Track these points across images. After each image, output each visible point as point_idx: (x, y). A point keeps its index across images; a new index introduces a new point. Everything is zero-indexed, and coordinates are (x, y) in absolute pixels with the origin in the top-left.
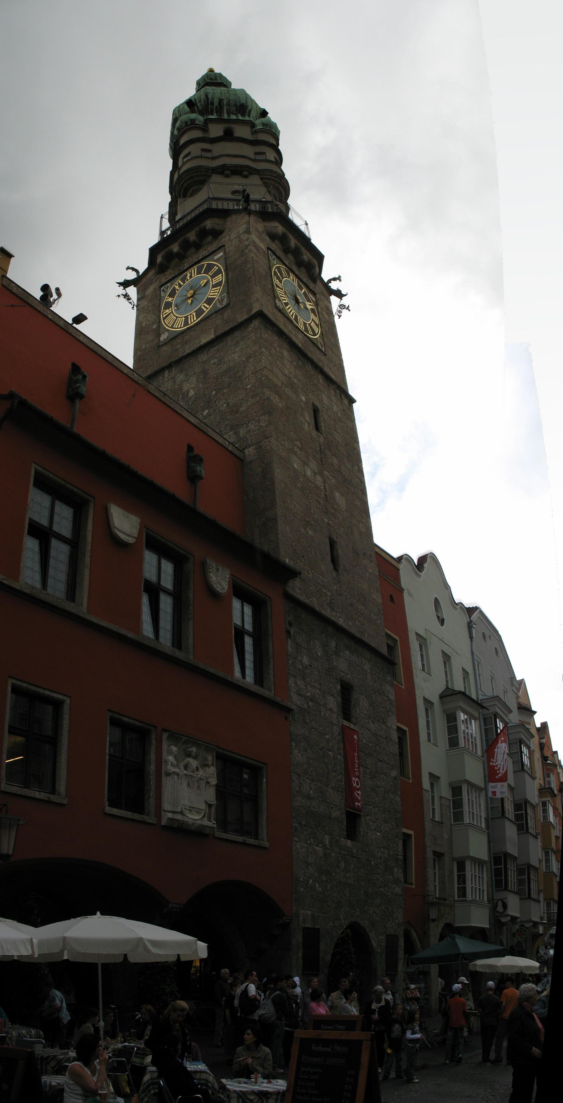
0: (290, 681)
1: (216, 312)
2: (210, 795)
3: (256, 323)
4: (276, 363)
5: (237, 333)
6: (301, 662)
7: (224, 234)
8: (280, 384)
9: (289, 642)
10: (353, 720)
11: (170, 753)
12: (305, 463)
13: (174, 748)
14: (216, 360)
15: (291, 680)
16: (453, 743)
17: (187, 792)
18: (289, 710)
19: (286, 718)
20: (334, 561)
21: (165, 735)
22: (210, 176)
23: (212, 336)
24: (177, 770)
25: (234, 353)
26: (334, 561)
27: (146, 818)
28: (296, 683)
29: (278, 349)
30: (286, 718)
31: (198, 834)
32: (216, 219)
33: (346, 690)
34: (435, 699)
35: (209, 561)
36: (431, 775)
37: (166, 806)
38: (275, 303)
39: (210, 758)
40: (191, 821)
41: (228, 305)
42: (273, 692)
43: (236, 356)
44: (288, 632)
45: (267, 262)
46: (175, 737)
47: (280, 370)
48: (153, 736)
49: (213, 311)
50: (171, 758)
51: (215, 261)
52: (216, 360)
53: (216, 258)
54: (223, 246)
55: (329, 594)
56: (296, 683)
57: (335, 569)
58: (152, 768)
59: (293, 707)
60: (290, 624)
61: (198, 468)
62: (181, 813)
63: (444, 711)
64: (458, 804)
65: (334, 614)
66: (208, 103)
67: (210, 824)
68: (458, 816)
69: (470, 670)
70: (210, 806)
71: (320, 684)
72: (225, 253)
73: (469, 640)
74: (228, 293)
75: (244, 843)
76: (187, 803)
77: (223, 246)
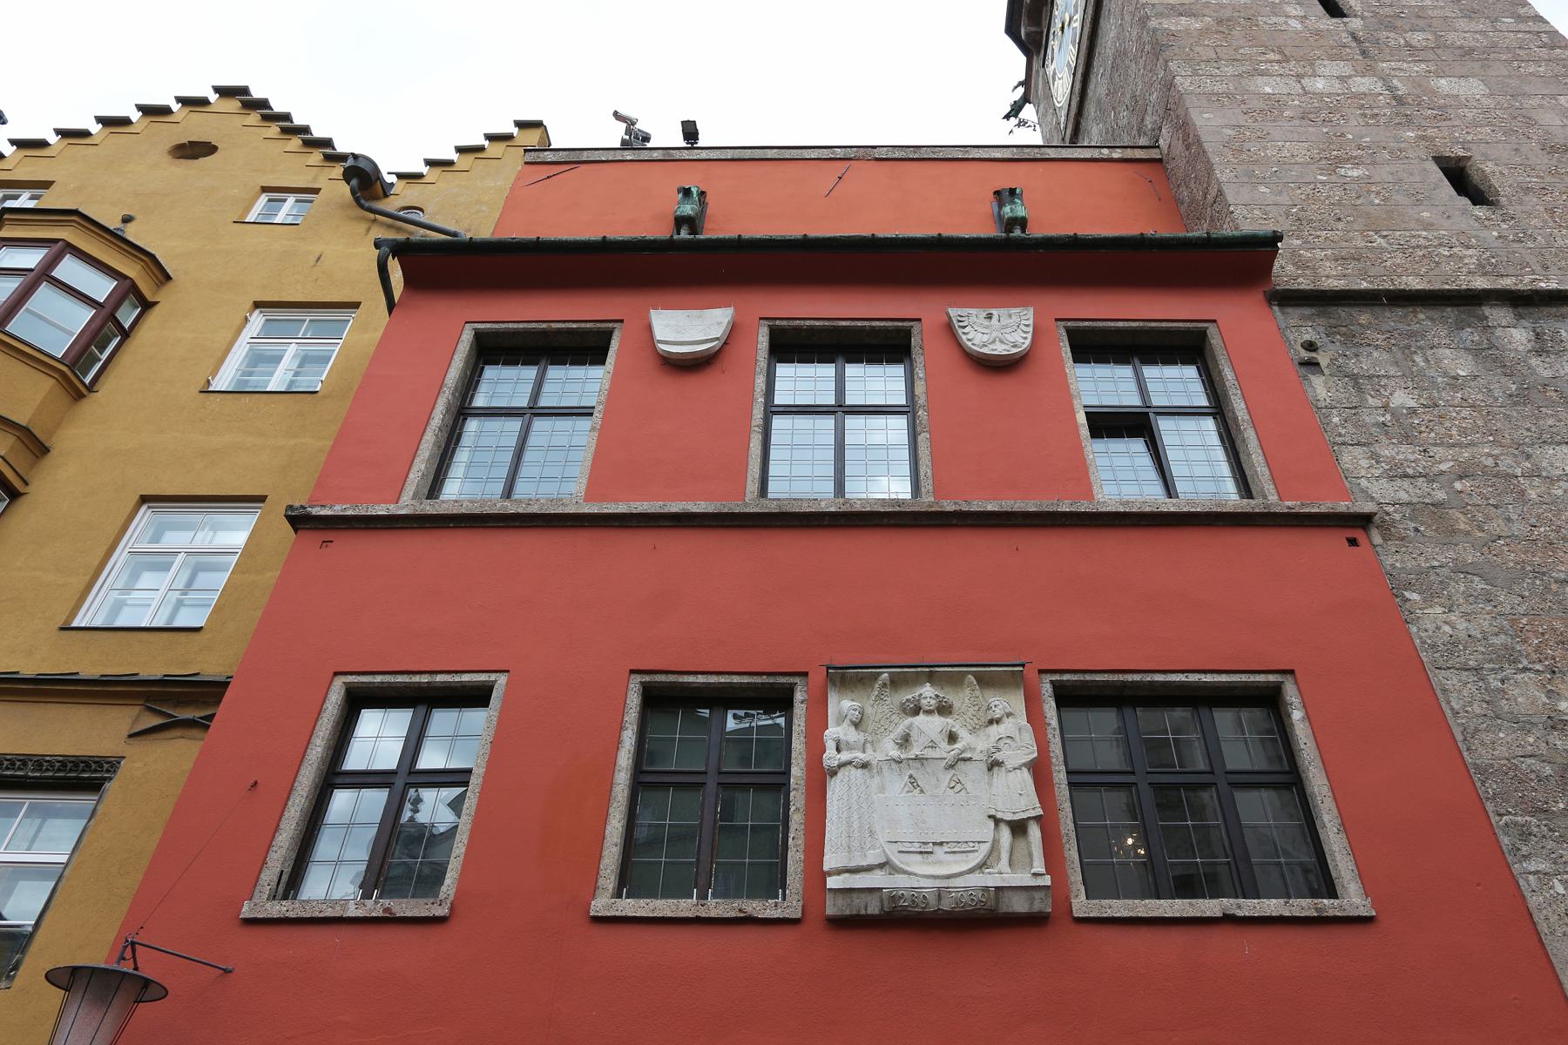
6: (1386, 407)
28: (1376, 457)
56: (1376, 457)
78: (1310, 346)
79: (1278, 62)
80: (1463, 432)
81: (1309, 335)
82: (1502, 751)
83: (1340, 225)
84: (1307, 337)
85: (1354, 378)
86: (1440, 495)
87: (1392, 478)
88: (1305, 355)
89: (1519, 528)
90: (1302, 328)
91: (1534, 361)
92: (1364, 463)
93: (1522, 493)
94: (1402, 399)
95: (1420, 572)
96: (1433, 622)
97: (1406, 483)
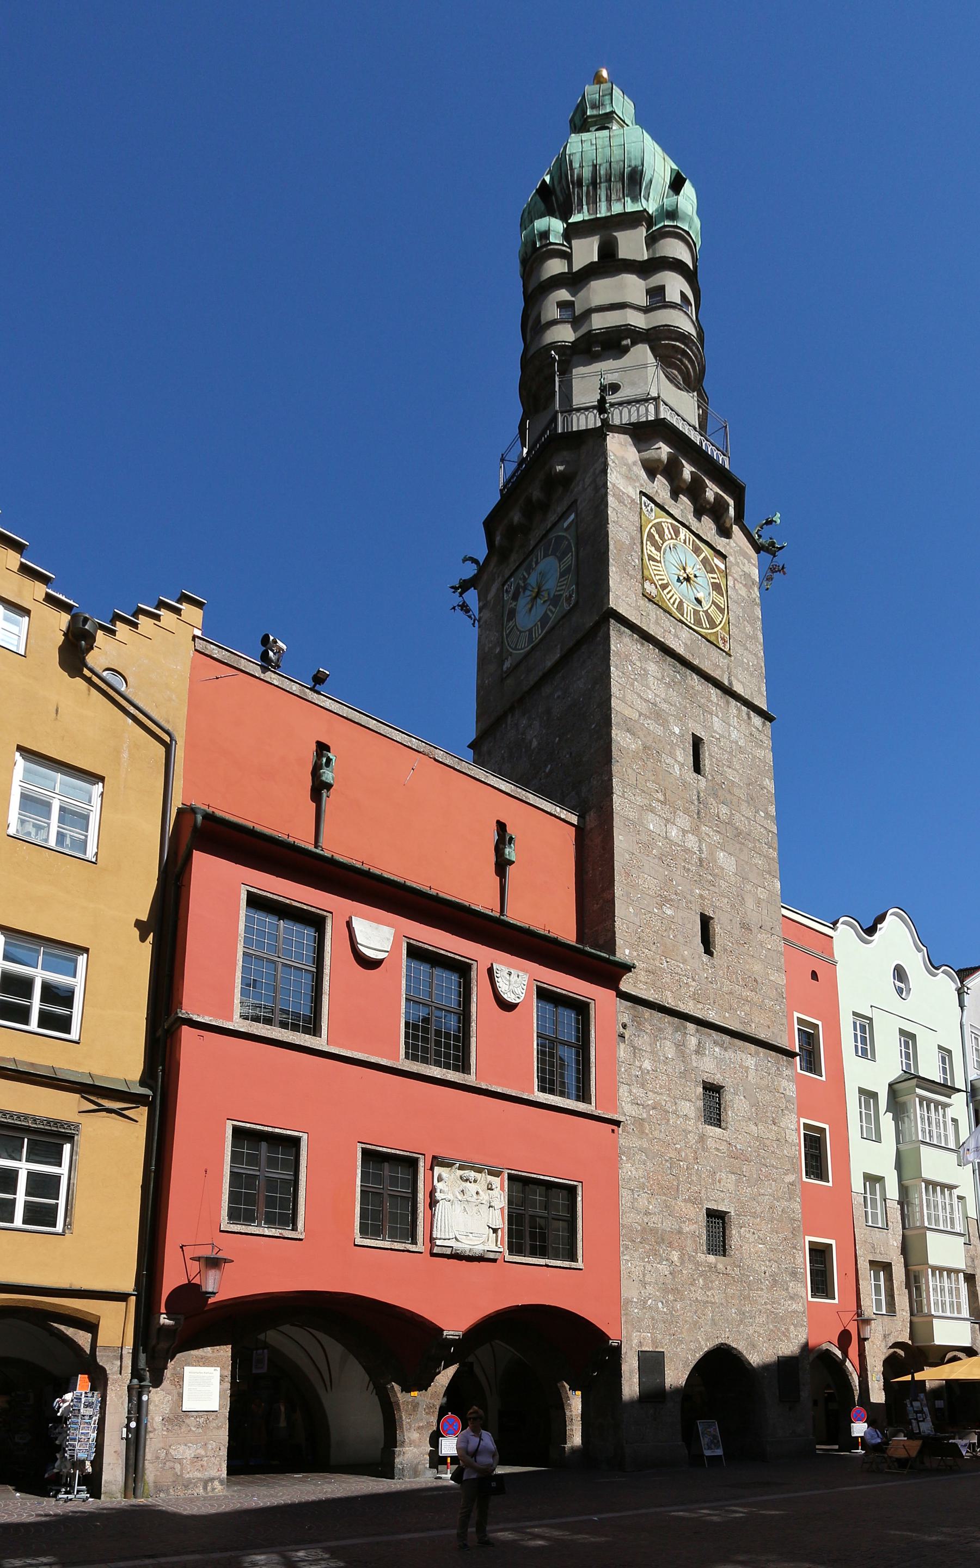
0: (621, 1090)
1: (563, 617)
4: (632, 685)
6: (640, 1067)
8: (635, 716)
14: (559, 693)
15: (623, 1091)
18: (617, 1123)
19: (613, 1131)
28: (630, 1092)
29: (638, 664)
30: (613, 1131)
38: (644, 589)
41: (577, 603)
42: (593, 1104)
44: (622, 1036)
45: (637, 519)
52: (559, 693)
53: (565, 525)
55: (693, 984)
56: (630, 1092)
57: (708, 951)
60: (624, 1026)
65: (700, 1006)
71: (670, 1090)
72: (576, 516)
74: (577, 585)
79: (659, 801)
80: (661, 1087)
81: (625, 1019)
82: (630, 1220)
83: (654, 948)
84: (625, 1020)
86: (645, 1116)
87: (632, 1104)
88: (622, 1030)
89: (662, 1136)
90: (624, 1012)
91: (693, 1057)
92: (626, 1094)
93: (668, 1120)
94: (647, 1065)
95: (629, 1148)
96: (628, 1170)
97: (635, 1107)
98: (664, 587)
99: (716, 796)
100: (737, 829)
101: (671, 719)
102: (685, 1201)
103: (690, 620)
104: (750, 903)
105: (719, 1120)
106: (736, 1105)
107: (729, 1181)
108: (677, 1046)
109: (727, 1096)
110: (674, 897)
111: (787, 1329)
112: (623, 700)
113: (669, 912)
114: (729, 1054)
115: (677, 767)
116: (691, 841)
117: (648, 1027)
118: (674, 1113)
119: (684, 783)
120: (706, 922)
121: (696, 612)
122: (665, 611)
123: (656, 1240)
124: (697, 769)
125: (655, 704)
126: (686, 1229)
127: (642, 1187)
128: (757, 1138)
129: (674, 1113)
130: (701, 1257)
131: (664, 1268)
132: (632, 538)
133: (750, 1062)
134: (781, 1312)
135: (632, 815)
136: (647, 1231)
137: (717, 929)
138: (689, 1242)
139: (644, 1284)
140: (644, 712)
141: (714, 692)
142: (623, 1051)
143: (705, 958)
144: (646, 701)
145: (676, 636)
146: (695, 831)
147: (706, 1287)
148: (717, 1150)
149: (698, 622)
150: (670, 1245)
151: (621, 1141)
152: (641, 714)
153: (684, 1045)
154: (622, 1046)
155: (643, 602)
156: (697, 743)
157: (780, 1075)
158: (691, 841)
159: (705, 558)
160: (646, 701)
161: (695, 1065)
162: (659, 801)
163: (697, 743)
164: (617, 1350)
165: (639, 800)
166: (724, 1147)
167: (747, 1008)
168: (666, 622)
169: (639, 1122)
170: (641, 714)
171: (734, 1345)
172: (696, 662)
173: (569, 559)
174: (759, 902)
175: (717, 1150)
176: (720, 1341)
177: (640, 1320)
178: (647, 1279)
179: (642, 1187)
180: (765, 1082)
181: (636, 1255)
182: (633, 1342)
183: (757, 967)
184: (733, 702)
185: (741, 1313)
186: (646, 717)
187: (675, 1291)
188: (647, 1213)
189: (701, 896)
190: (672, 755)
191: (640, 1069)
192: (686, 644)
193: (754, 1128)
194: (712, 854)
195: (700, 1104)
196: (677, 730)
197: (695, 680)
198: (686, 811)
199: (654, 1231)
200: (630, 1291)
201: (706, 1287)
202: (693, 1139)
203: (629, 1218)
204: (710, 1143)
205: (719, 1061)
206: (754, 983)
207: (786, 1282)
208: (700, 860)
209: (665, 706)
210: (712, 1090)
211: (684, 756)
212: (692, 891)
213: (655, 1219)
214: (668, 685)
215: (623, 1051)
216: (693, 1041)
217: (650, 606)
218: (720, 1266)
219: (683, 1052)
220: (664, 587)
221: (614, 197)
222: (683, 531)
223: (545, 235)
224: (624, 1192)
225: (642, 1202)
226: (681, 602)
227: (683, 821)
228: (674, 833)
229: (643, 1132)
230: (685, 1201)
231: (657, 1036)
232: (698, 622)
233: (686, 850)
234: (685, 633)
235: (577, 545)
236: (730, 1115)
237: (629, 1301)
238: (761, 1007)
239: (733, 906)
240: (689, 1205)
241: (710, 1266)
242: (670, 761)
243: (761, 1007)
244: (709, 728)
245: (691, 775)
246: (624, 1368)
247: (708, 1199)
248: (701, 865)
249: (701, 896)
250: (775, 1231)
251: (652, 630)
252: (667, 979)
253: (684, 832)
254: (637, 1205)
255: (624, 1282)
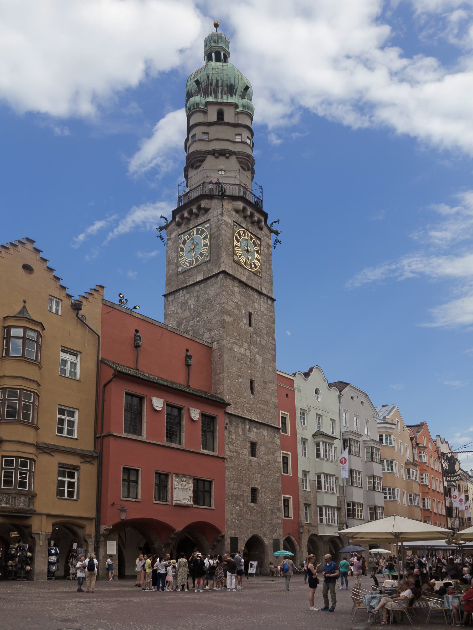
2: (191, 494)
3: (221, 276)
5: (213, 279)
7: (211, 211)
8: (231, 309)
9: (226, 431)
10: (257, 456)
11: (176, 481)
12: (241, 346)
13: (177, 480)
15: (226, 447)
16: (318, 456)
17: (182, 492)
18: (224, 458)
20: (252, 389)
21: (174, 475)
22: (206, 157)
23: (202, 278)
24: (178, 487)
25: (212, 290)
26: (252, 389)
27: (167, 503)
28: (228, 447)
31: (186, 507)
32: (206, 200)
33: (253, 445)
34: (309, 437)
35: (191, 408)
36: (303, 471)
37: (174, 499)
39: (190, 481)
40: (183, 503)
41: (210, 260)
43: (211, 292)
44: (226, 428)
46: (177, 475)
47: (232, 300)
48: (170, 476)
49: (203, 262)
50: (176, 483)
51: (206, 228)
54: (210, 220)
57: (252, 393)
58: (169, 486)
59: (226, 457)
61: (190, 361)
62: (180, 500)
63: (315, 442)
64: (319, 482)
66: (209, 84)
67: (190, 503)
68: (320, 488)
69: (336, 418)
70: (191, 497)
73: (338, 403)
74: (210, 253)
75: (204, 508)
76: (182, 497)
77: (210, 220)
78: (227, 424)
79: (238, 339)
85: (230, 431)
94: (233, 437)
98: (240, 256)
99: (256, 333)
100: (263, 345)
101: (242, 308)
102: (245, 484)
103: (248, 267)
104: (266, 373)
105: (255, 454)
106: (261, 449)
107: (258, 476)
108: (243, 429)
109: (258, 447)
110: (242, 374)
111: (276, 529)
112: (227, 304)
113: (240, 380)
114: (259, 431)
115: (244, 325)
116: (248, 353)
117: (234, 423)
118: (241, 453)
119: (246, 331)
120: (252, 382)
121: (251, 264)
122: (240, 266)
123: (236, 498)
124: (250, 325)
125: (237, 303)
126: (245, 495)
127: (232, 480)
128: (268, 461)
129: (241, 453)
130: (249, 504)
131: (238, 508)
132: (230, 240)
133: (266, 433)
134: (274, 523)
135: (229, 346)
136: (233, 495)
137: (256, 385)
138: (246, 499)
139: (232, 514)
140: (234, 306)
141: (256, 295)
142: (226, 433)
143: (252, 396)
144: (234, 302)
145: (244, 274)
146: (249, 348)
147: (251, 515)
148: (255, 466)
149: (251, 268)
150: (240, 500)
151: (226, 465)
152: (232, 308)
153: (245, 429)
154: (226, 431)
155: (234, 264)
156: (250, 314)
157: (275, 437)
158: (248, 353)
159: (254, 241)
160: (234, 302)
161: (248, 435)
162: (238, 339)
163: (250, 314)
164: (223, 537)
165: (232, 340)
166: (257, 465)
167: (265, 413)
168: (241, 270)
169: (231, 457)
170: (232, 308)
171: (259, 535)
172: (250, 284)
173: (207, 241)
174: (269, 372)
175: (255, 466)
176: (255, 533)
177: (231, 526)
178: (233, 512)
179: (232, 480)
180: (270, 440)
181: (230, 504)
182: (229, 533)
183: (268, 397)
184: (262, 299)
185: (262, 523)
186: (235, 309)
187: (241, 516)
188: (233, 489)
189: (251, 373)
190: (242, 321)
191: (232, 440)
192: (247, 277)
193: (266, 457)
194: (254, 356)
195: (250, 449)
196: (244, 311)
197: (250, 291)
198: (246, 342)
199: (235, 495)
200: (228, 516)
201: (251, 515)
202: (247, 462)
203: (228, 491)
204: (253, 464)
205: (256, 433)
206: (267, 403)
207: (276, 513)
208: (251, 359)
209: (240, 303)
210: (253, 445)
211: (246, 321)
212: (248, 372)
213: (235, 491)
214: (241, 294)
215: (226, 433)
216: (247, 427)
217: (236, 265)
218: (255, 507)
219: (244, 431)
220: (240, 256)
221: (223, 93)
222: (246, 232)
223: (198, 104)
224: (226, 482)
225: (232, 486)
226: (246, 261)
227: (245, 345)
228: (242, 350)
229: (232, 461)
230: (245, 484)
231: (236, 427)
232: (251, 268)
233: (246, 356)
234: (247, 273)
235: (210, 237)
236: (258, 453)
237: (228, 520)
238: (269, 412)
239: (261, 375)
240: (246, 486)
241: (252, 507)
242: (241, 323)
243: (269, 412)
244: (254, 308)
245: (248, 328)
246: (226, 542)
247: (252, 484)
248: (251, 361)
249: (251, 373)
250: (273, 494)
251: (237, 275)
252: (239, 405)
253: (246, 350)
254: (231, 487)
255: (226, 513)
